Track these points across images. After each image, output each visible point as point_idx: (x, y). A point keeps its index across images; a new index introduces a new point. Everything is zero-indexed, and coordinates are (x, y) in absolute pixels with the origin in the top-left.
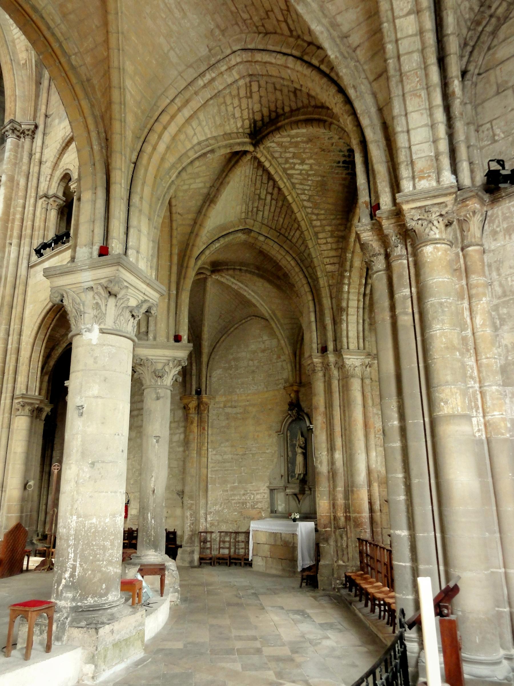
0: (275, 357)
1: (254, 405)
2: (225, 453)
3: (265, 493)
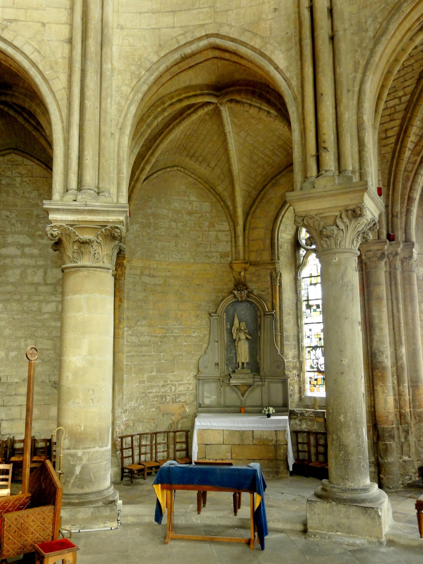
0: (207, 224)
1: (176, 277)
2: (142, 334)
3: (189, 384)
